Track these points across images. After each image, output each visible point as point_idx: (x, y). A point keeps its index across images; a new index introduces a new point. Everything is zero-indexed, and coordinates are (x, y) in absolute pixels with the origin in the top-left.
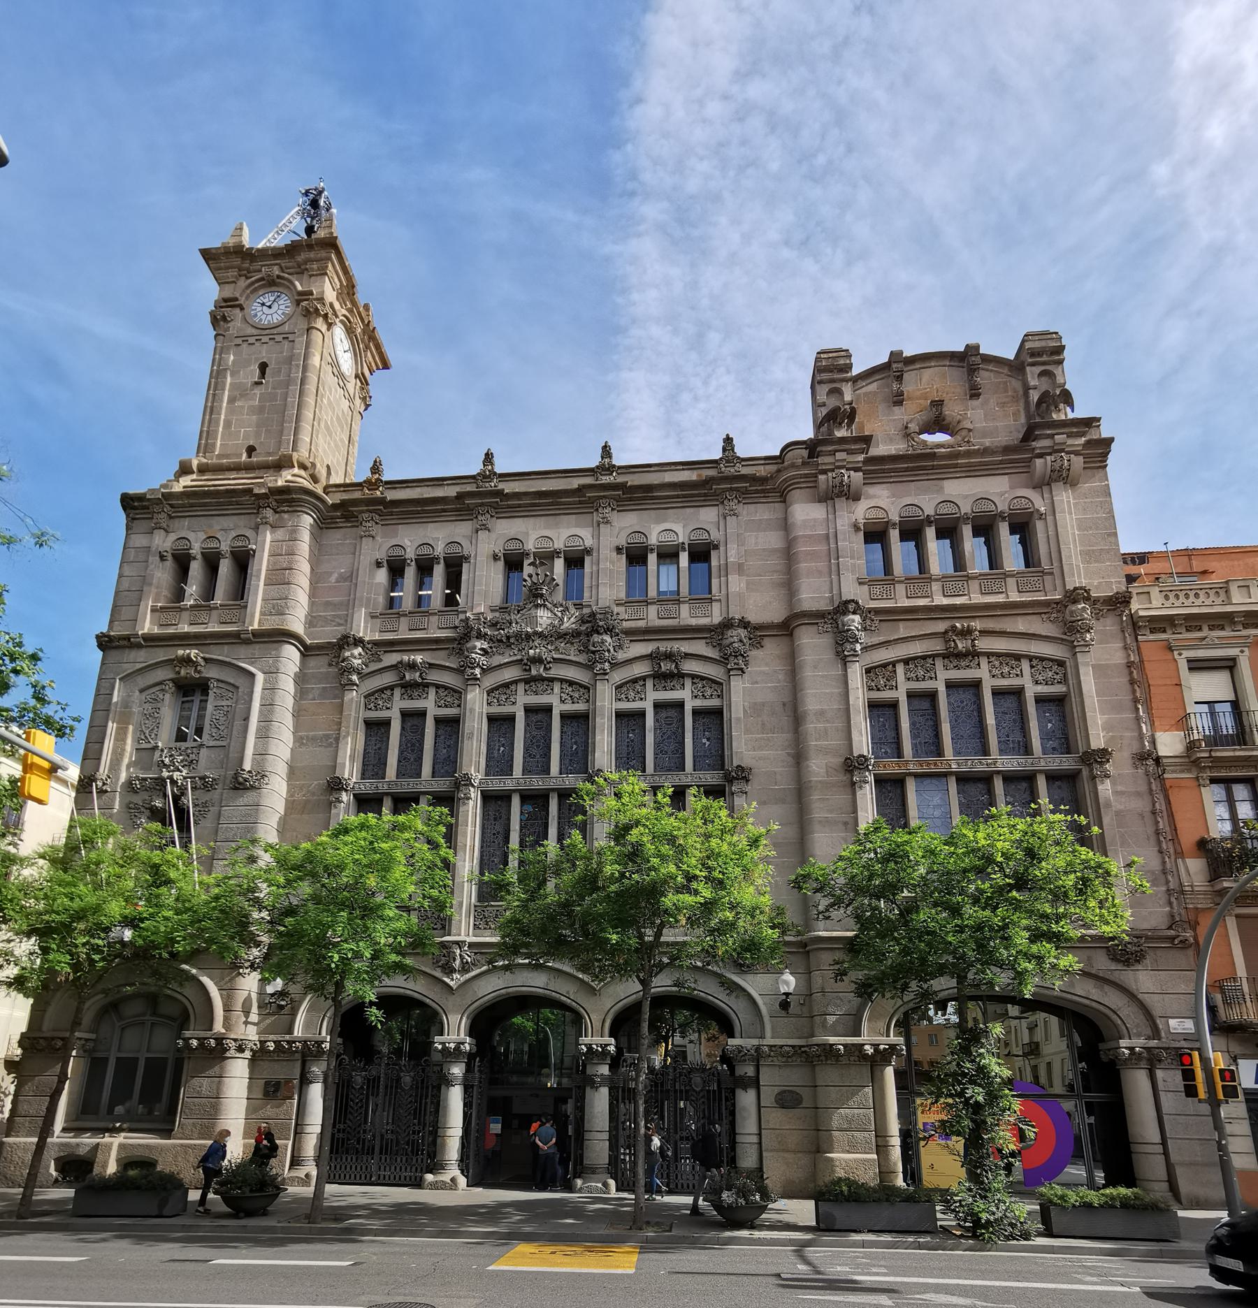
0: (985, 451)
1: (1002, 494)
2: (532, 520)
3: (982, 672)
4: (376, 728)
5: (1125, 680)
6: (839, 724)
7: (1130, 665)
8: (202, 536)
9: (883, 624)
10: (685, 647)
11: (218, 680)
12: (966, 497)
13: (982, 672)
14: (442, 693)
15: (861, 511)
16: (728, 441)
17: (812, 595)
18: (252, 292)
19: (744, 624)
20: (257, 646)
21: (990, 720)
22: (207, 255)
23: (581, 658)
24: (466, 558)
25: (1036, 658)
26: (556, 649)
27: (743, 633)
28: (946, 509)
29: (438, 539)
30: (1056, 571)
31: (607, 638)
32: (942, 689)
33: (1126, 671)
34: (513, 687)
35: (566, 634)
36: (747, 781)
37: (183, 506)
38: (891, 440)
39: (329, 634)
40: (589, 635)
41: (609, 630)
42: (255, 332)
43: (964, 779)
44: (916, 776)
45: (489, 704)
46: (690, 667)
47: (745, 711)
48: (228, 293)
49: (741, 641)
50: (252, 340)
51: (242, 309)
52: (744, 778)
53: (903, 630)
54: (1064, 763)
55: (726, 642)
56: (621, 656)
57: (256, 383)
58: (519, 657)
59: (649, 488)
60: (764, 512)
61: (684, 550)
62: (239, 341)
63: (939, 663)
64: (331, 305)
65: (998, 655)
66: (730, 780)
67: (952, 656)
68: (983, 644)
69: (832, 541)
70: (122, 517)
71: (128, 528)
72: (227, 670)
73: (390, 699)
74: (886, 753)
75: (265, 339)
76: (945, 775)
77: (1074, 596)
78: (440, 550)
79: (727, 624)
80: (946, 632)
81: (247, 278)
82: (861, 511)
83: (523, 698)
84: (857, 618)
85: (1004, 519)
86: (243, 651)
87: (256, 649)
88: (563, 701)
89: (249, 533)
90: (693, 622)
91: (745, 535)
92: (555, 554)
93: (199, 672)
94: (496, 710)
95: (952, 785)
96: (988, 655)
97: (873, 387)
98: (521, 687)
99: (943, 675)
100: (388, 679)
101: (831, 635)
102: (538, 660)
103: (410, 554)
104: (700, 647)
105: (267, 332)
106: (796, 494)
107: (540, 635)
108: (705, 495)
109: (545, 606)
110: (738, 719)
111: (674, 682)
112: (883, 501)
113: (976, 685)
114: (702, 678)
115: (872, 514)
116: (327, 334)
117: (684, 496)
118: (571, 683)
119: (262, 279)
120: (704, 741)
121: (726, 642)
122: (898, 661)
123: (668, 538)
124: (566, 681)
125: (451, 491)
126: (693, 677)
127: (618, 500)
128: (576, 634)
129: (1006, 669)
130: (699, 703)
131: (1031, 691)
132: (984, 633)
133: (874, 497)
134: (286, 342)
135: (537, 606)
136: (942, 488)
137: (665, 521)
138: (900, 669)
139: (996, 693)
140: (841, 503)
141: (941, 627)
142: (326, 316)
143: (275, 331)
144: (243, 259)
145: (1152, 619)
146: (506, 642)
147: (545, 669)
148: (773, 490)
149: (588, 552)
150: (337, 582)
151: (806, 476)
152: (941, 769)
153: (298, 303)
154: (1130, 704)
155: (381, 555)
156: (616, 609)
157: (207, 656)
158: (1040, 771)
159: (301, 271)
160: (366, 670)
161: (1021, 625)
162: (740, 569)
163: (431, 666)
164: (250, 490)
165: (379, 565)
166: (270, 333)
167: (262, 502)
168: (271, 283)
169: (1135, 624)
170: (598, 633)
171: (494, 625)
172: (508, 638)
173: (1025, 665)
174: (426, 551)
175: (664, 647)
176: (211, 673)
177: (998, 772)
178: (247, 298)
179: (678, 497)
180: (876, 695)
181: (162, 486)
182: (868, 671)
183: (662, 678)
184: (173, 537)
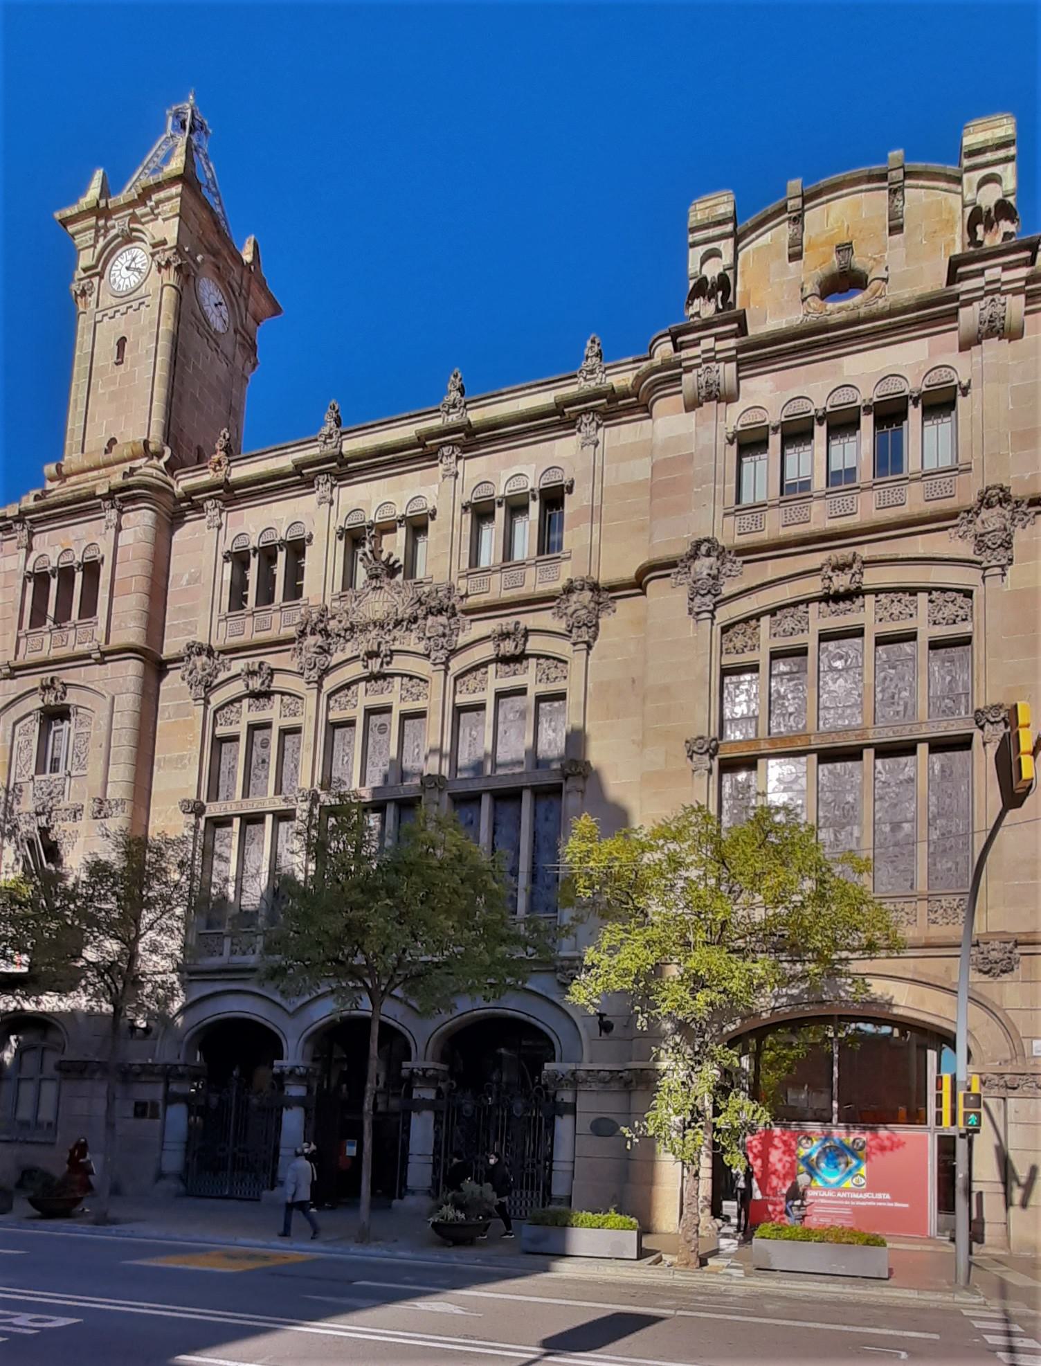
23: (421, 647)
42: (115, 301)
75: (123, 308)
88: (402, 699)
105: (126, 299)
115: (749, 418)
124: (406, 675)
136: (841, 367)
143: (132, 297)
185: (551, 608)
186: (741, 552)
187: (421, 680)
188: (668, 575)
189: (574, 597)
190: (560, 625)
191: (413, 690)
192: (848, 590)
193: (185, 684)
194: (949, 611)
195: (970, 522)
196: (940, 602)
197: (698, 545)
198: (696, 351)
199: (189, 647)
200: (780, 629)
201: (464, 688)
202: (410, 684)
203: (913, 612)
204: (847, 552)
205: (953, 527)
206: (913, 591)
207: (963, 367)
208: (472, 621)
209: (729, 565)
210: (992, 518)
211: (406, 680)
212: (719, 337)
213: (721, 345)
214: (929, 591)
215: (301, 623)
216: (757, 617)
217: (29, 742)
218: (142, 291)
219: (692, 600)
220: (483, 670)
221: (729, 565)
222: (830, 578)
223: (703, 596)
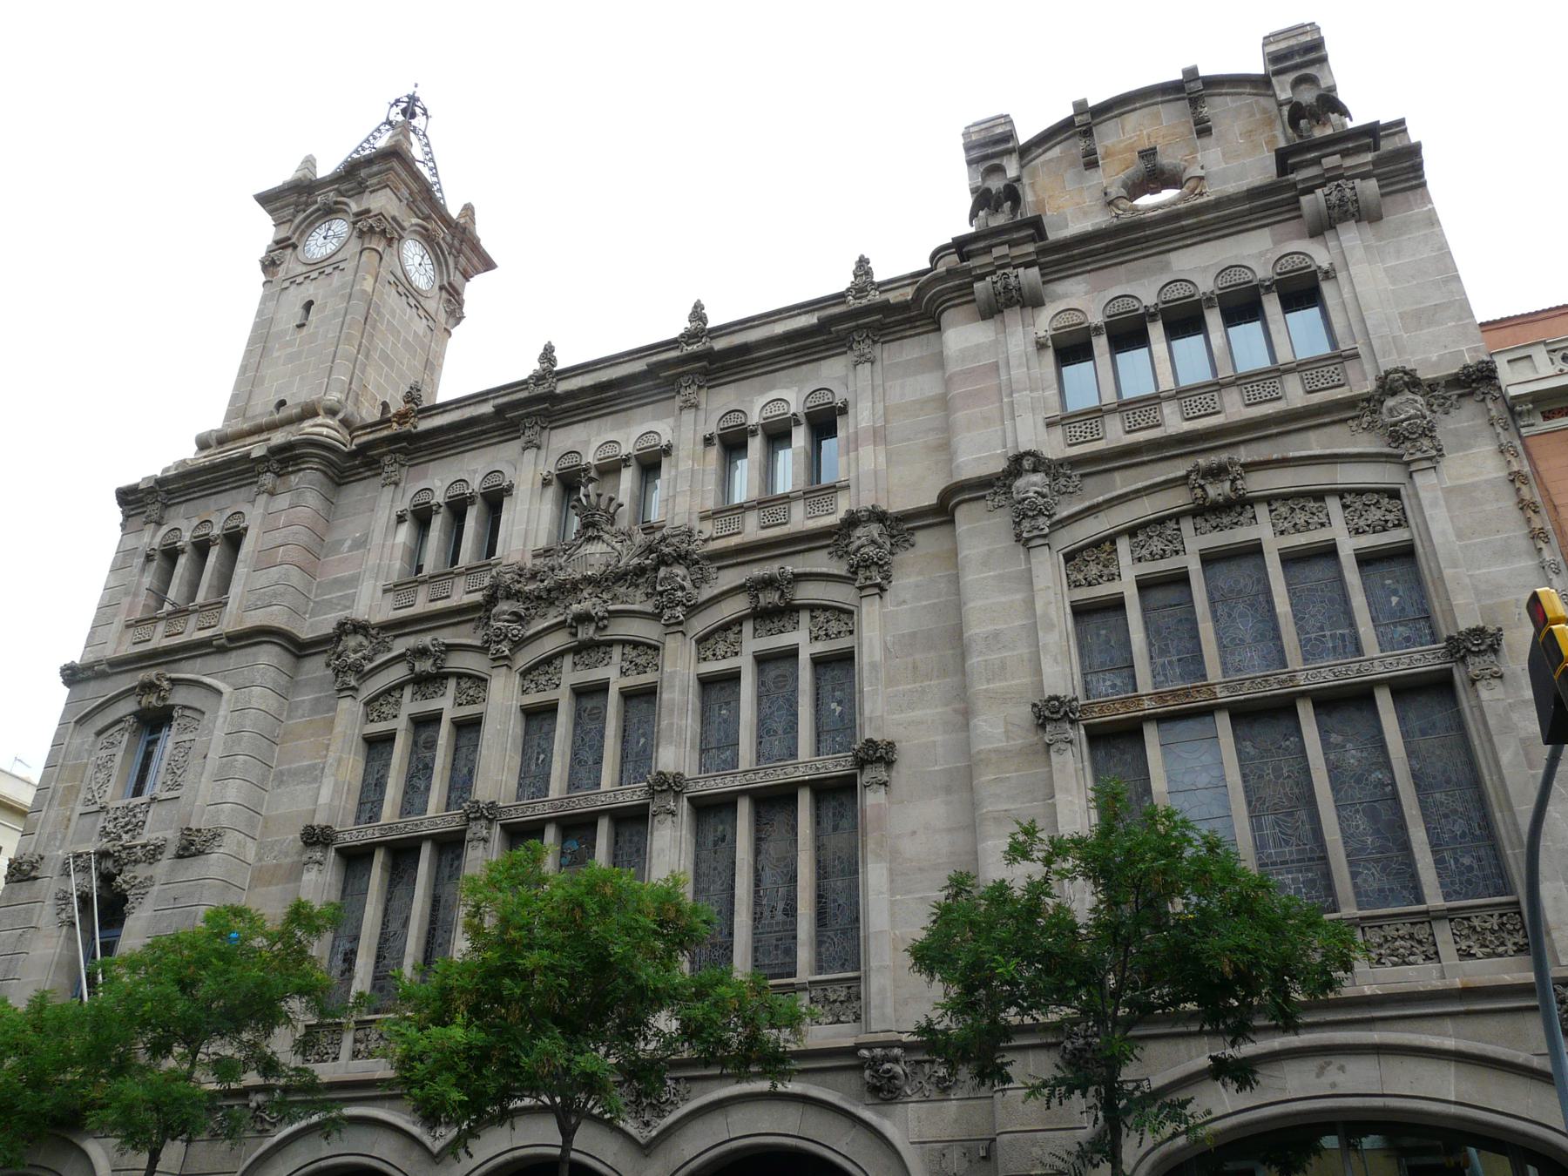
0: (1230, 200)
1: (1261, 254)
2: (595, 422)
3: (1261, 529)
4: (377, 745)
5: (1509, 503)
6: (1023, 650)
7: (1515, 478)
8: (196, 521)
9: (1089, 482)
10: (793, 566)
11: (185, 707)
12: (1205, 269)
13: (1261, 529)
14: (465, 684)
15: (1044, 322)
16: (863, 266)
17: (978, 455)
18: (308, 227)
19: (879, 516)
20: (234, 654)
21: (1282, 604)
22: (265, 199)
23: (649, 607)
24: (508, 490)
25: (1350, 491)
26: (615, 598)
27: (875, 529)
28: (1176, 293)
29: (475, 472)
30: (1362, 350)
31: (679, 570)
32: (1194, 566)
33: (1508, 490)
34: (557, 662)
35: (626, 574)
36: (889, 764)
37: (179, 490)
38: (1085, 214)
39: (324, 624)
40: (656, 569)
41: (681, 558)
42: (305, 269)
43: (1246, 714)
44: (1160, 719)
45: (524, 692)
46: (808, 593)
47: (886, 649)
48: (283, 235)
49: (873, 542)
52: (880, 759)
53: (1122, 483)
54: (1421, 660)
55: (853, 547)
56: (706, 593)
57: (301, 326)
58: (561, 618)
59: (745, 349)
60: (910, 350)
61: (798, 423)
62: (287, 284)
63: (1187, 526)
64: (394, 218)
65: (1285, 497)
66: (861, 763)
67: (1204, 511)
68: (1257, 483)
69: (1003, 372)
70: (116, 514)
71: (123, 526)
72: (197, 690)
73: (398, 703)
74: (1114, 686)
75: (314, 275)
76: (1208, 711)
77: (1397, 382)
78: (476, 485)
79: (853, 520)
80: (1187, 477)
82: (1044, 322)
83: (571, 674)
84: (1038, 478)
85: (1268, 289)
86: (215, 662)
87: (233, 659)
88: (623, 673)
89: (245, 508)
90: (812, 524)
91: (870, 387)
92: (625, 462)
93: (164, 699)
94: (534, 698)
95: (1223, 722)
96: (1269, 500)
97: (1056, 152)
98: (568, 661)
99: (1196, 541)
100: (399, 672)
101: (1008, 509)
102: (584, 618)
103: (439, 497)
104: (820, 562)
106: (947, 318)
107: (589, 580)
108: (826, 342)
109: (599, 538)
110: (874, 666)
111: (785, 621)
112: (1083, 299)
113: (1254, 550)
114: (825, 608)
117: (796, 350)
118: (636, 645)
120: (834, 705)
121: (853, 547)
122: (1120, 534)
123: (775, 411)
124: (629, 642)
125: (487, 408)
126: (812, 608)
127: (706, 373)
128: (640, 571)
129: (1300, 518)
130: (821, 647)
131: (1348, 547)
132: (1250, 467)
133: (1065, 296)
135: (590, 539)
137: (772, 388)
138: (1123, 545)
139: (1291, 559)
140: (1013, 316)
141: (1179, 469)
142: (384, 231)
144: (300, 194)
145: (1537, 398)
146: (547, 599)
147: (598, 629)
148: (921, 317)
149: (667, 451)
150: (351, 549)
151: (959, 288)
152: (1200, 700)
153: (354, 223)
154: (1523, 543)
155: (404, 504)
156: (697, 526)
157: (174, 676)
158: (1380, 683)
159: (361, 189)
160: (369, 666)
161: (1315, 443)
162: (879, 436)
163: (451, 648)
164: (248, 455)
165: (401, 519)
166: (322, 268)
167: (260, 468)
168: (330, 212)
169: (1516, 410)
170: (667, 565)
171: (534, 576)
172: (549, 591)
173: (1333, 505)
174: (457, 490)
175: (771, 569)
176: (179, 697)
177: (1303, 694)
179: (788, 352)
180: (1084, 594)
181: (166, 470)
182: (1069, 557)
183: (765, 617)
184: (164, 529)
185: (828, 546)
186: (1075, 462)
187: (649, 646)
188: (984, 497)
189: (859, 532)
190: (839, 568)
191: (638, 661)
192: (1228, 499)
193: (329, 672)
194: (1375, 515)
195: (1373, 412)
196: (1358, 505)
197: (1018, 459)
198: (986, 259)
199: (341, 625)
200: (1144, 552)
201: (709, 653)
202: (634, 653)
203: (1324, 520)
204: (1223, 457)
205: (1352, 418)
206: (1319, 496)
207: (1320, 255)
208: (719, 568)
209: (1062, 481)
210: (1406, 406)
211: (628, 649)
212: (1012, 244)
213: (1016, 251)
214: (1341, 494)
215: (492, 586)
216: (1112, 539)
217: (111, 757)
218: (339, 257)
219: (1019, 524)
220: (736, 629)
221: (1062, 481)
222: (1201, 487)
223: (1033, 517)
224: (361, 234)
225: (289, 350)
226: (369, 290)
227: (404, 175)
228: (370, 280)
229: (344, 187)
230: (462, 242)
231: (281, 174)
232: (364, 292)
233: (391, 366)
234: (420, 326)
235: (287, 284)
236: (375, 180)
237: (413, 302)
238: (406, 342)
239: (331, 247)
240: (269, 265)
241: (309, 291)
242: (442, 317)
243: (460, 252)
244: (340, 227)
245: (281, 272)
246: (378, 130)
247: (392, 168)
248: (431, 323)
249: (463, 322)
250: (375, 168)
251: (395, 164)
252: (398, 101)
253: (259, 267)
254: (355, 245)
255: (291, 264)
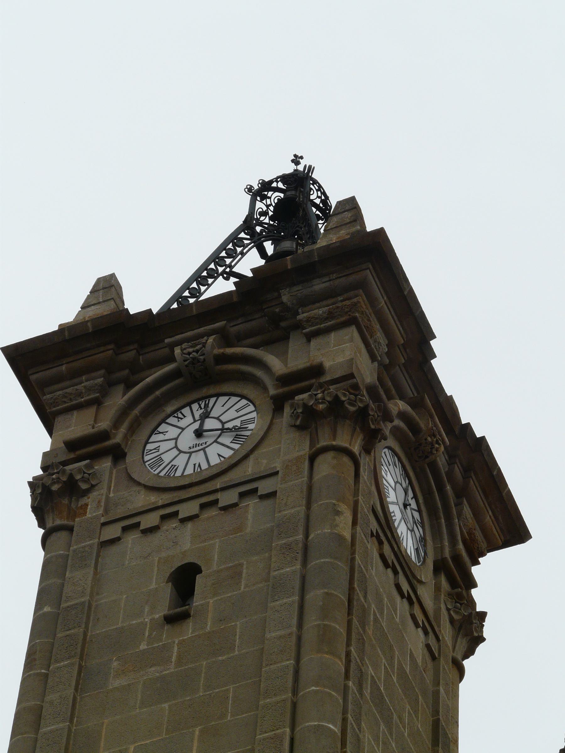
42: (154, 499)
50: (151, 520)
51: (118, 454)
62: (114, 531)
75: (186, 510)
81: (129, 386)
116: (365, 461)
119: (176, 374)
134: (252, 503)
142: (363, 413)
143: (218, 484)
153: (278, 404)
159: (277, 334)
166: (204, 492)
168: (200, 382)
178: (133, 429)
224: (308, 420)
225: (153, 672)
226: (347, 535)
227: (382, 302)
228: (348, 516)
229: (238, 327)
230: (467, 470)
231: (55, 309)
232: (340, 538)
233: (389, 723)
234: (416, 640)
235: (114, 531)
236: (320, 311)
237: (405, 587)
238: (402, 674)
239: (218, 453)
240: (53, 497)
241: (181, 543)
242: (446, 632)
243: (462, 493)
244: (233, 411)
245: (93, 507)
246: (234, 239)
247: (362, 285)
248: (432, 641)
249: (481, 649)
250: (319, 286)
251: (370, 276)
252: (266, 186)
253: (25, 498)
254: (288, 447)
255: (108, 490)
